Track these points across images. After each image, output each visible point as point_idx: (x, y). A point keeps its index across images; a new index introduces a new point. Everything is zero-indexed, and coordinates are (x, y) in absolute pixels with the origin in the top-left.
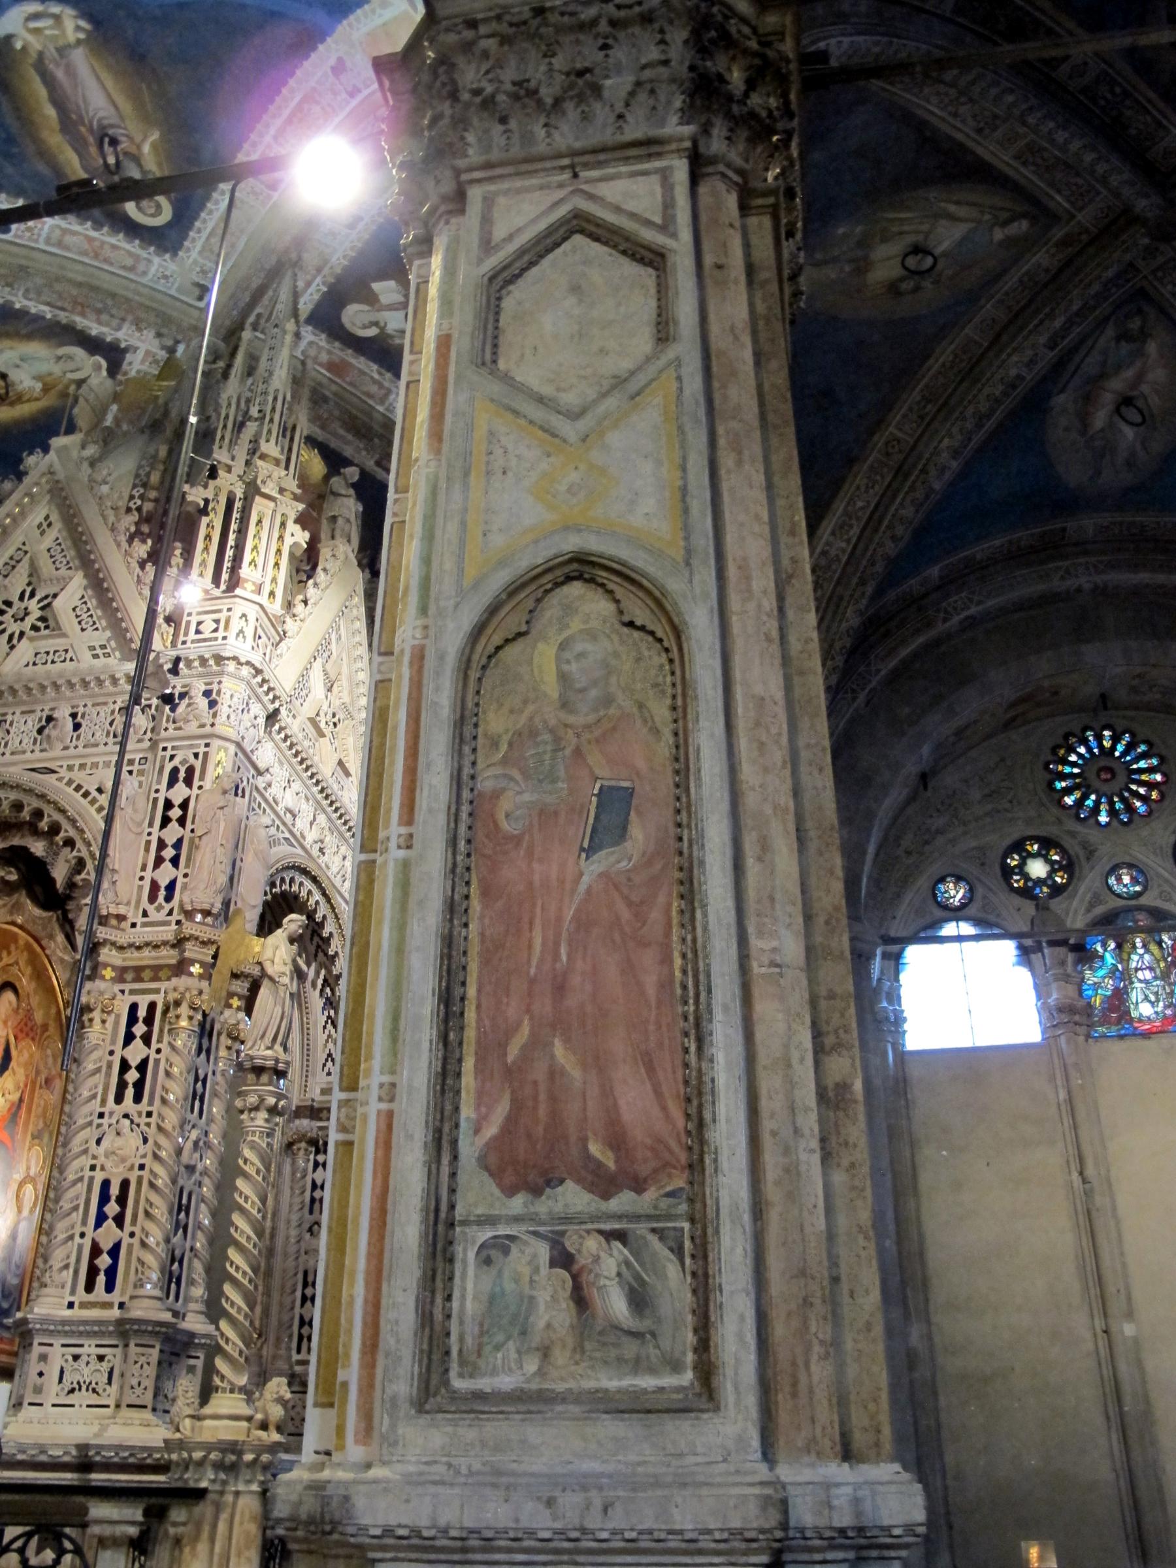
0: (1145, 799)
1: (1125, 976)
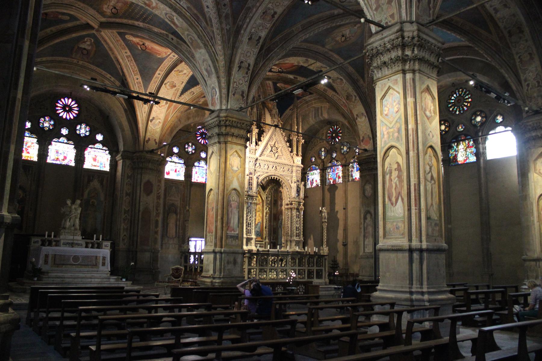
0: (466, 106)
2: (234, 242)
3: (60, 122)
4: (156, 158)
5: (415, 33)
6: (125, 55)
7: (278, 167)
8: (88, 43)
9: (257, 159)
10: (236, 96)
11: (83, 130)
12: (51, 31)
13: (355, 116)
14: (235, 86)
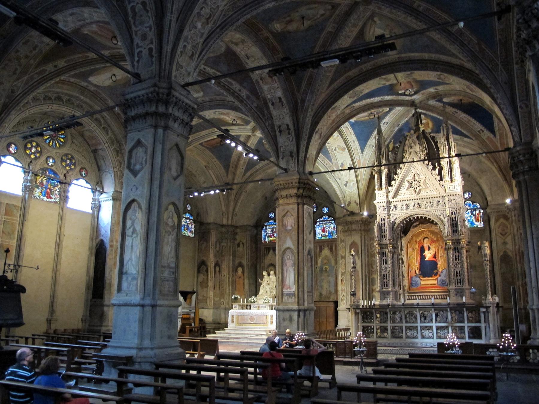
2: (290, 300)
4: (357, 218)
7: (421, 204)
10: (284, 159)
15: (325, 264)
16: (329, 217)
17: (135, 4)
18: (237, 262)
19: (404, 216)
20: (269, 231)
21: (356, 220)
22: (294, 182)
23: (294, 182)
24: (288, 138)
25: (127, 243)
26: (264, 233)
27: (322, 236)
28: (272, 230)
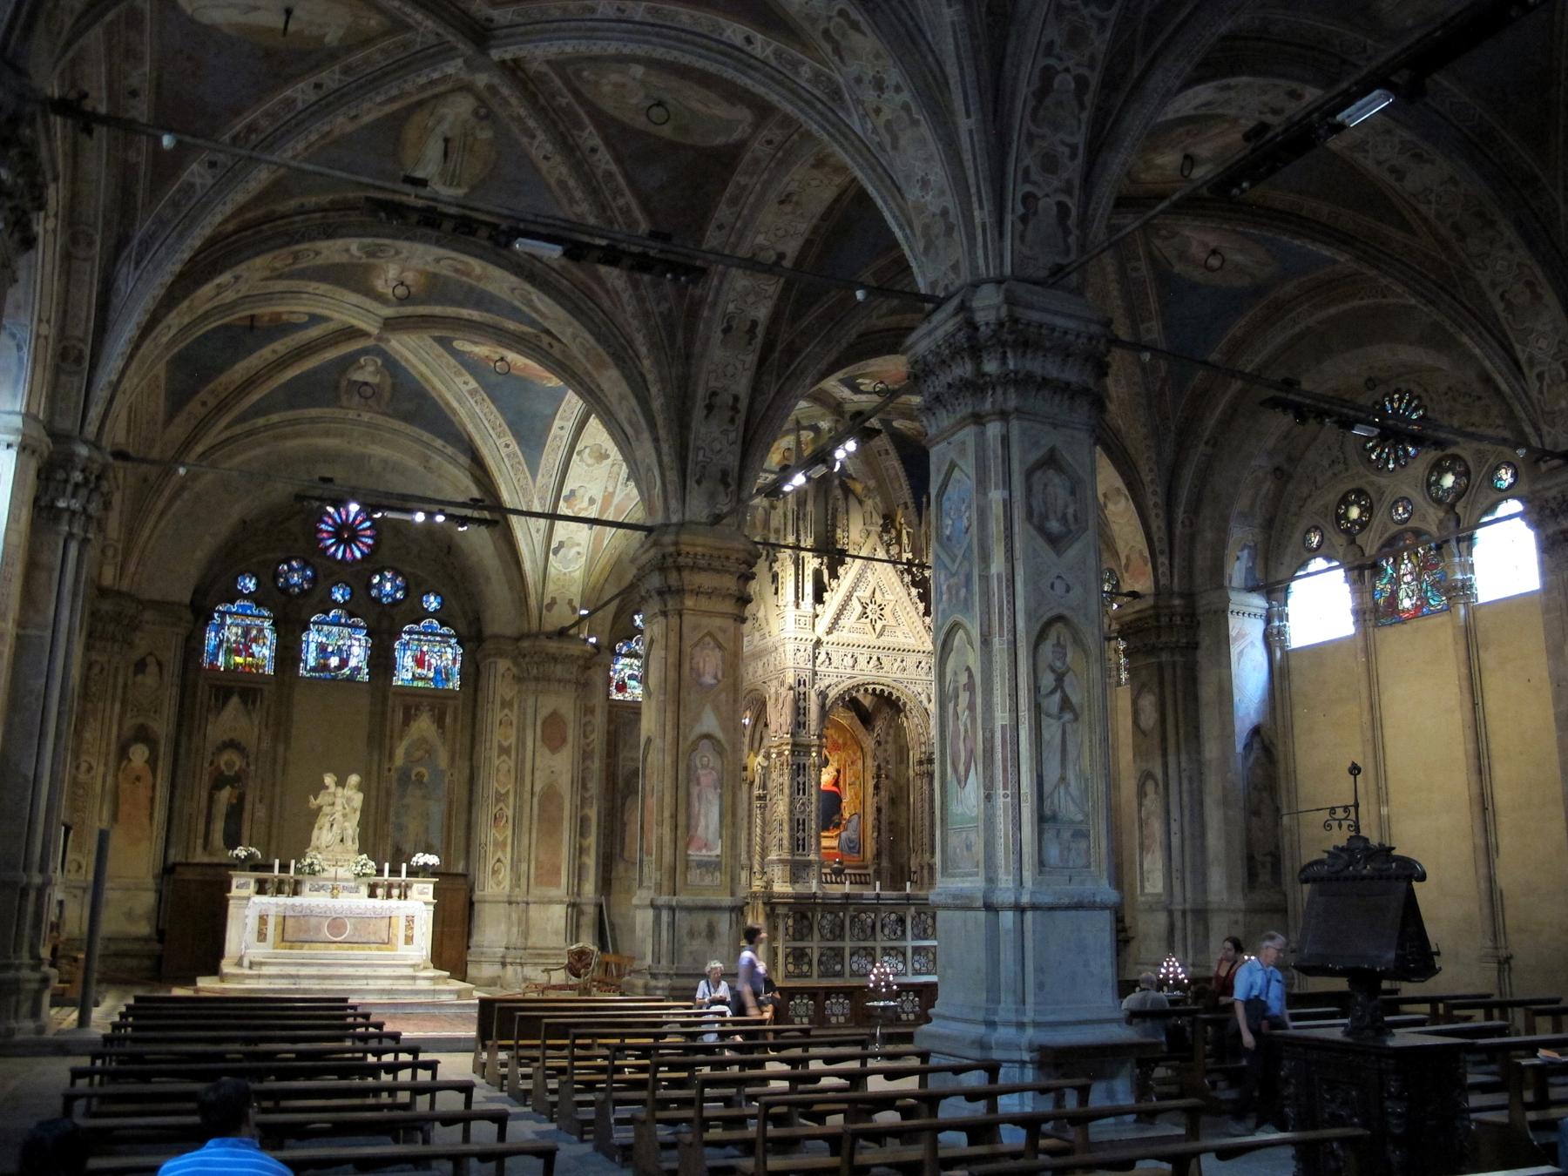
1: (1396, 581)
2: (708, 880)
3: (326, 572)
4: (574, 649)
5: (1004, 311)
6: (465, 388)
7: (884, 660)
8: (371, 368)
9: (818, 643)
10: (705, 484)
11: (387, 586)
12: (274, 351)
13: (1101, 499)
14: (701, 457)
15: (419, 761)
16: (442, 624)
17: (1060, 67)
18: (130, 722)
19: (848, 684)
20: (232, 633)
21: (570, 652)
22: (733, 557)
23: (733, 557)
24: (725, 432)
25: (1046, 735)
26: (211, 638)
27: (414, 678)
28: (246, 632)
